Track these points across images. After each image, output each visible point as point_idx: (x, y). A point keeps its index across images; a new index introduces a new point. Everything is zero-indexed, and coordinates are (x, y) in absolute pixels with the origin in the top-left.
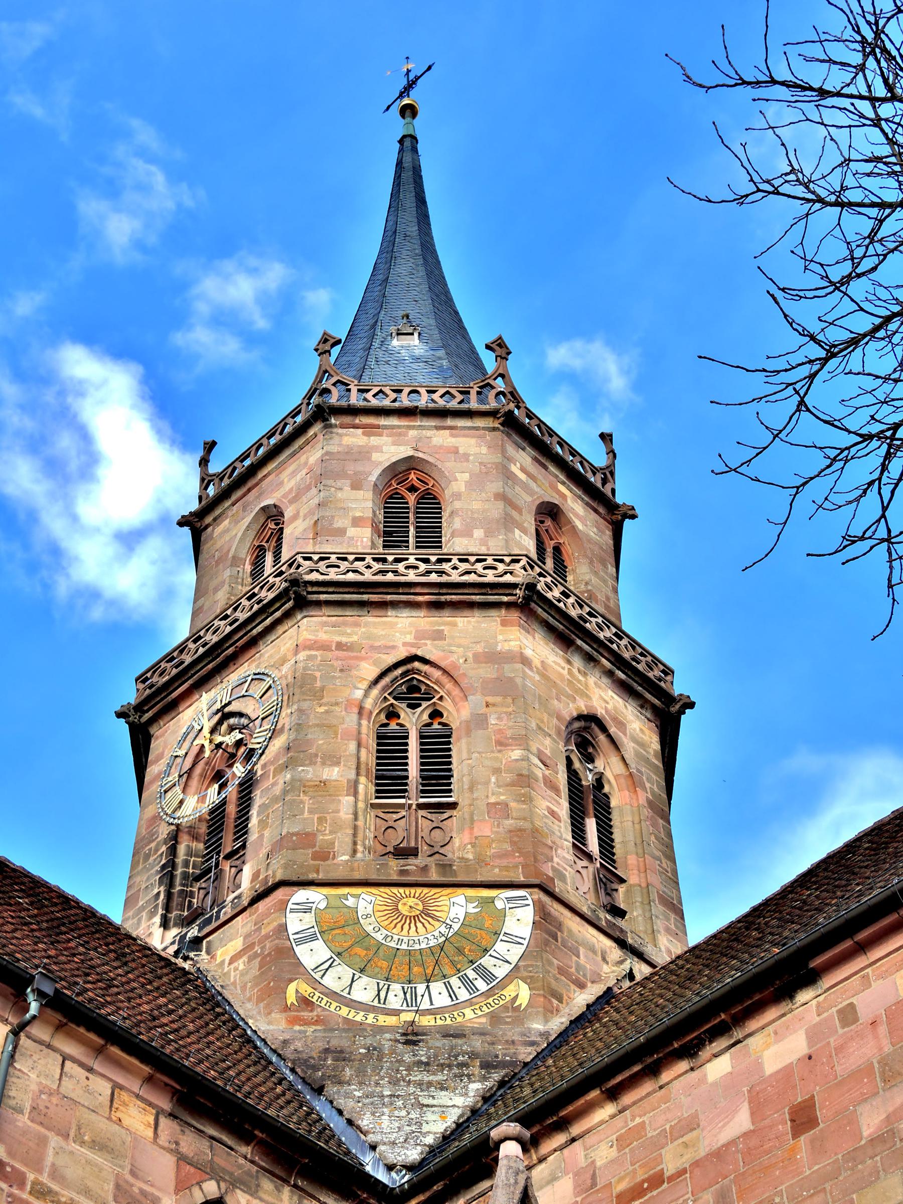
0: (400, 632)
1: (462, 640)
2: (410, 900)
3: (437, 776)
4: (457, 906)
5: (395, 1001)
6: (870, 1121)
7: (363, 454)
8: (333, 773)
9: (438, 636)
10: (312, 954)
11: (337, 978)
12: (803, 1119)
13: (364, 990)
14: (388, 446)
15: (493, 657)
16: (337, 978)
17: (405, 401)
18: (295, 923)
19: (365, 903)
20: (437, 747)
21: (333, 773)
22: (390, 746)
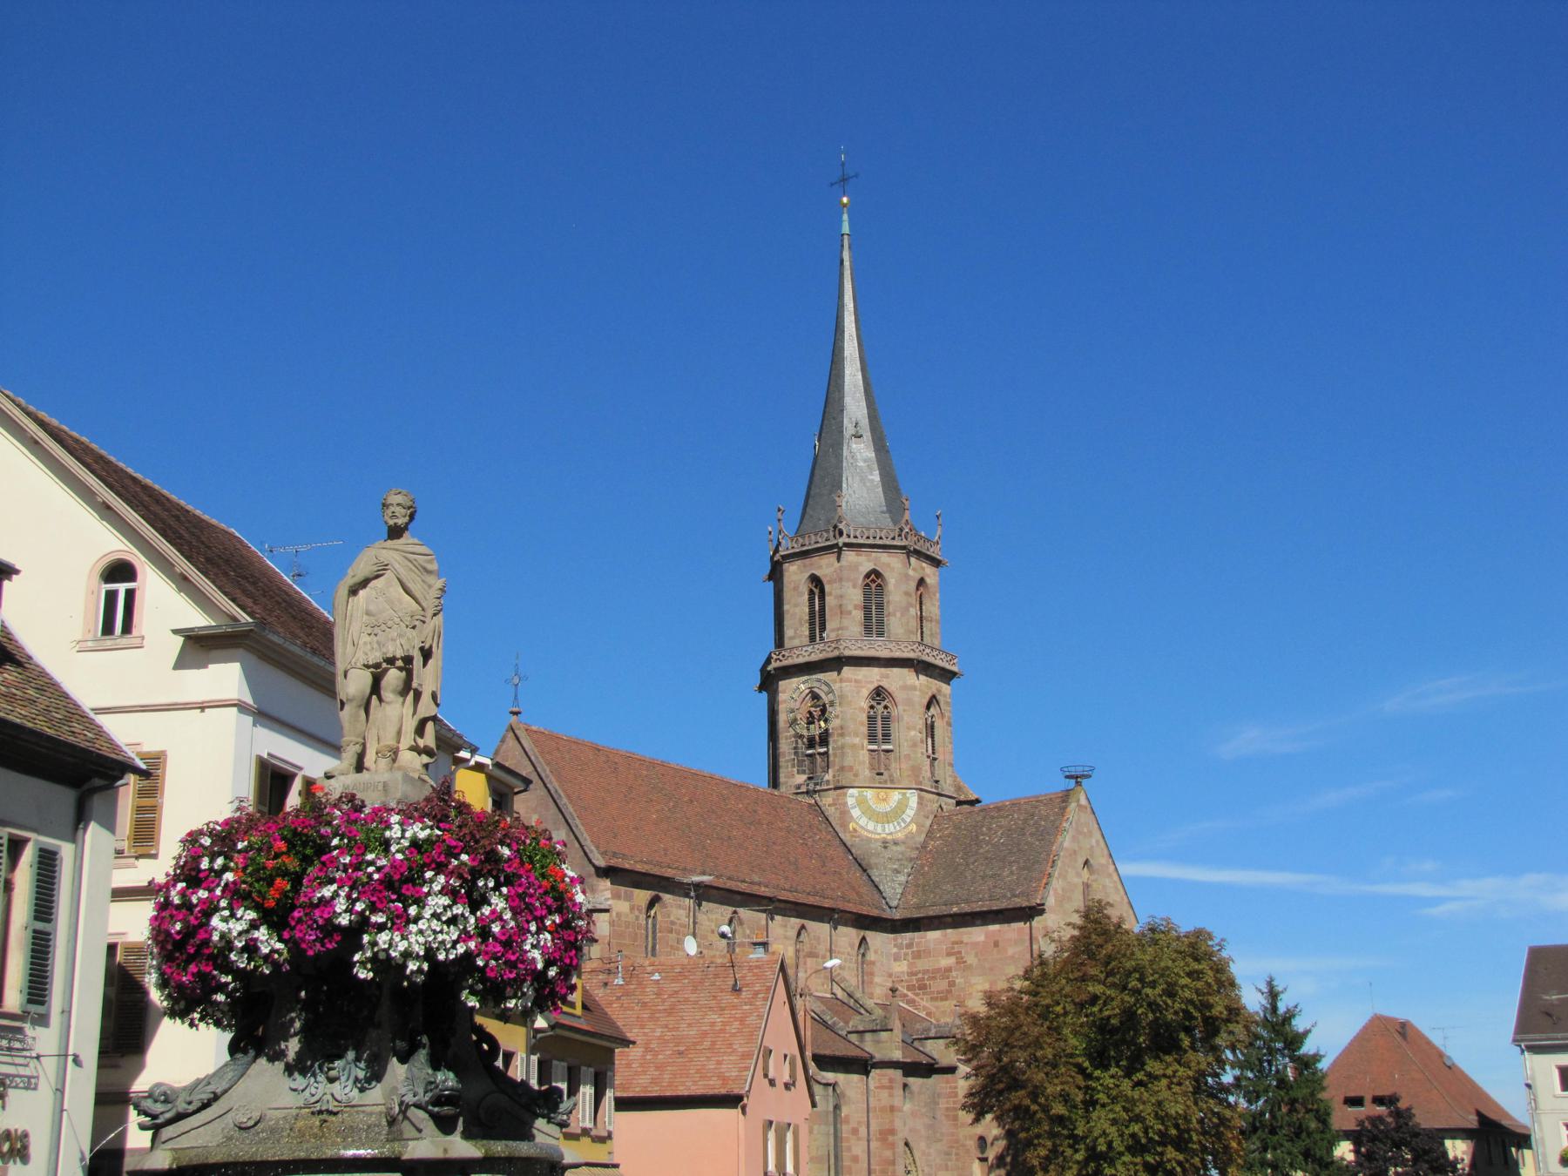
0: (873, 676)
1: (899, 680)
2: (882, 793)
3: (887, 737)
4: (896, 796)
5: (879, 830)
6: (1010, 951)
7: (855, 567)
8: (857, 740)
9: (887, 676)
10: (856, 813)
11: (863, 821)
12: (996, 944)
13: (871, 826)
14: (863, 562)
15: (905, 688)
16: (863, 821)
17: (871, 541)
18: (850, 801)
19: (869, 793)
20: (886, 719)
21: (857, 740)
22: (871, 719)
